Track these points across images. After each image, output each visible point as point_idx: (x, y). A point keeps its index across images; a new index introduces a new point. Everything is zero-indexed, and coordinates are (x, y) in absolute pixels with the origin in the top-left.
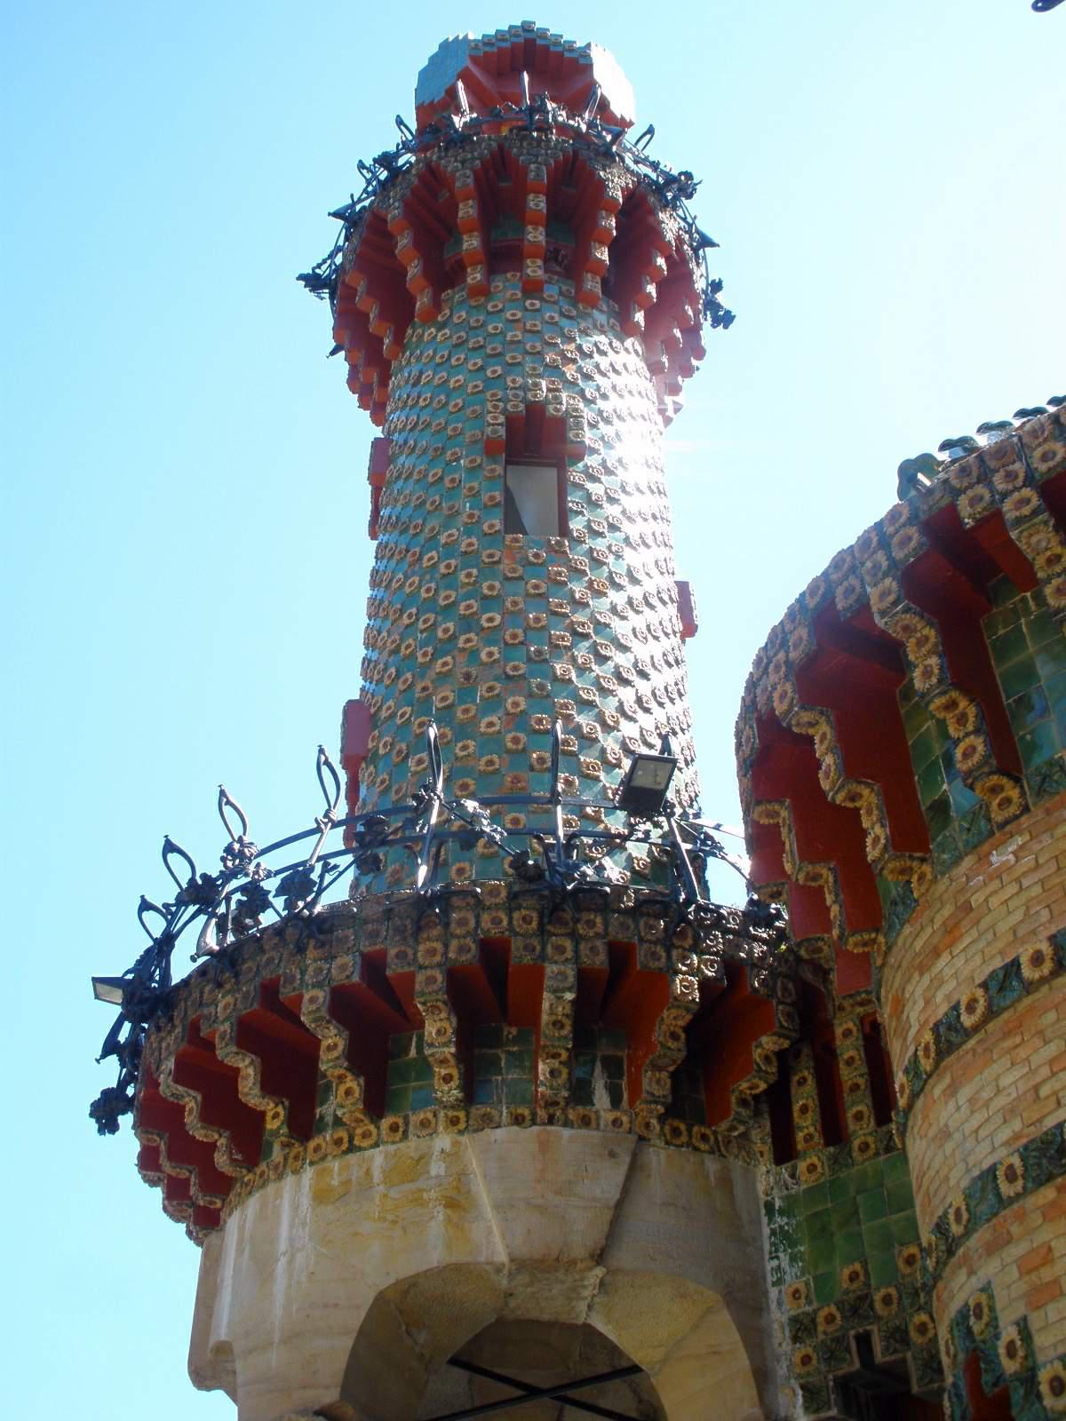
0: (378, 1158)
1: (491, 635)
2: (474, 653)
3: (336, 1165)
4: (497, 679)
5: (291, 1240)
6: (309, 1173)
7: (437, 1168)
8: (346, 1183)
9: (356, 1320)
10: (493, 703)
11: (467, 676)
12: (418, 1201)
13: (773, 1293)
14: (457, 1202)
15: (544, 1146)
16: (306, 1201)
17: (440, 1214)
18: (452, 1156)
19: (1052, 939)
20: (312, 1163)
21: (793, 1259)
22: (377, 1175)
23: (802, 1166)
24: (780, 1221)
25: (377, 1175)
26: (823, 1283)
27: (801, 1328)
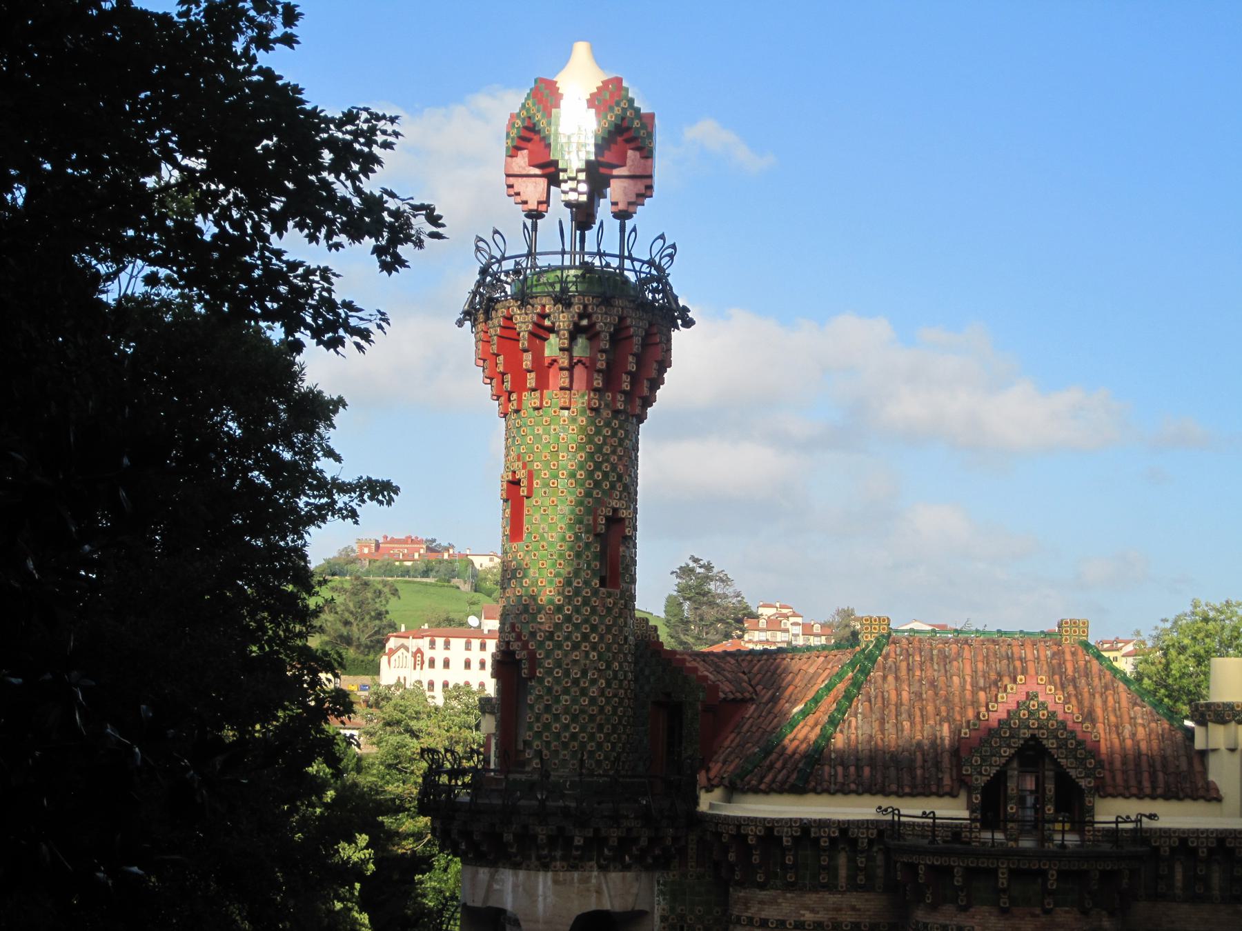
0: (576, 875)
1: (594, 647)
2: (587, 653)
3: (561, 874)
4: (595, 669)
5: (544, 892)
6: (550, 874)
7: (594, 881)
8: (565, 880)
9: (571, 922)
10: (593, 682)
11: (585, 665)
12: (588, 890)
13: (656, 907)
14: (599, 892)
15: (624, 878)
16: (550, 883)
17: (595, 894)
18: (598, 877)
19: (795, 921)
20: (552, 871)
21: (664, 899)
22: (576, 880)
23: (671, 874)
24: (661, 887)
25: (576, 880)
26: (672, 909)
27: (664, 919)
